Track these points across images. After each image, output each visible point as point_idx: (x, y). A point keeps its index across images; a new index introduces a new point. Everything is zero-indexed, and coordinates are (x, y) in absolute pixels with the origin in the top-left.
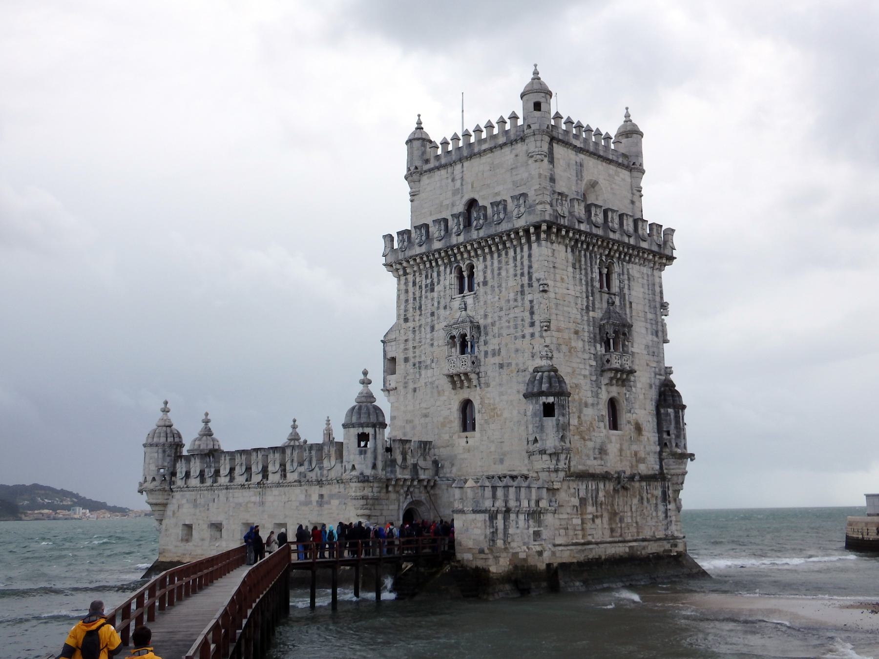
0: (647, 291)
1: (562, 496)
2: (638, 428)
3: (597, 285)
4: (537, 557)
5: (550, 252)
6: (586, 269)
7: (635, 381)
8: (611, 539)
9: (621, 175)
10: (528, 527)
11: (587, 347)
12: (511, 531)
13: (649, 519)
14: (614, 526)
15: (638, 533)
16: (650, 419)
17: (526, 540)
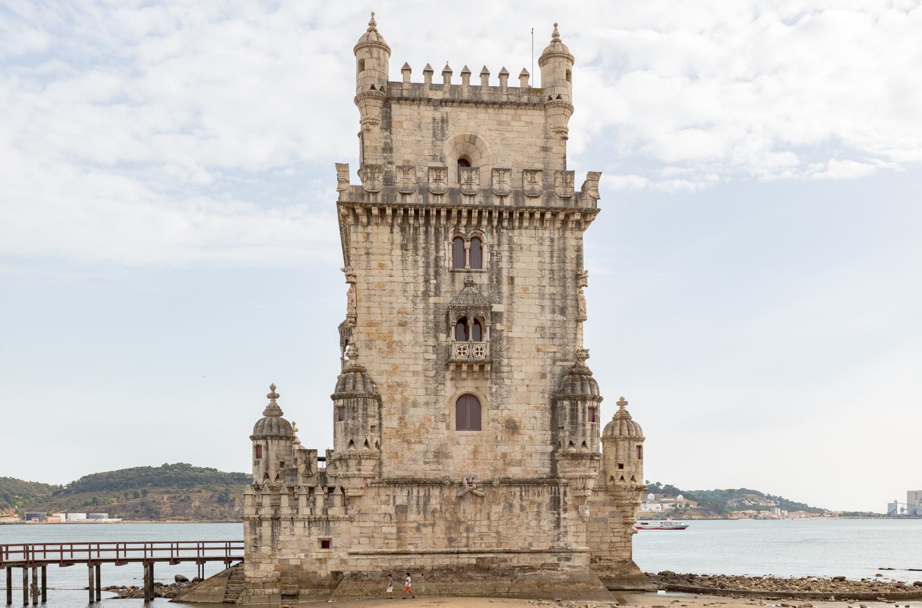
0: (547, 260)
1: (368, 502)
2: (512, 427)
3: (448, 263)
4: (318, 564)
5: (361, 237)
6: (426, 249)
8: (445, 550)
9: (523, 118)
10: (310, 535)
11: (421, 339)
12: (281, 538)
13: (522, 529)
14: (453, 536)
15: (499, 544)
16: (538, 415)
17: (306, 547)
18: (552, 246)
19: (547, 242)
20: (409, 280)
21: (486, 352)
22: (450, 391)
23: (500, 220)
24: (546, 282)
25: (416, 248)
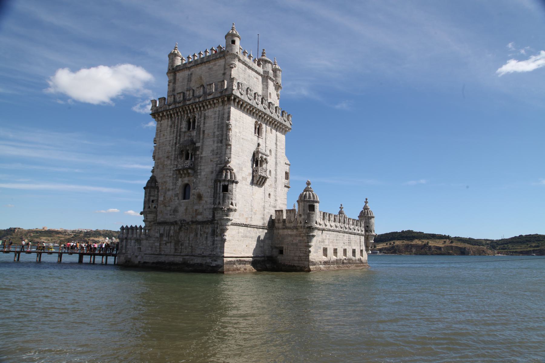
0: (217, 120)
2: (200, 197)
6: (177, 125)
7: (201, 172)
9: (218, 64)
11: (173, 162)
12: (128, 247)
14: (177, 247)
15: (192, 252)
16: (209, 191)
18: (219, 114)
19: (217, 113)
20: (171, 139)
21: (189, 164)
22: (180, 183)
23: (200, 108)
24: (216, 130)
25: (174, 126)
